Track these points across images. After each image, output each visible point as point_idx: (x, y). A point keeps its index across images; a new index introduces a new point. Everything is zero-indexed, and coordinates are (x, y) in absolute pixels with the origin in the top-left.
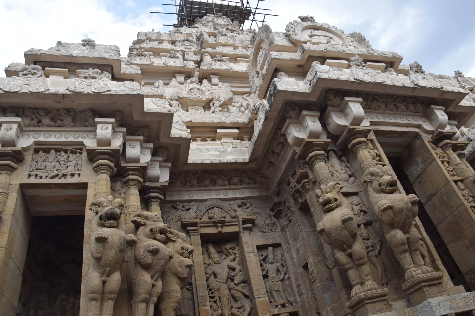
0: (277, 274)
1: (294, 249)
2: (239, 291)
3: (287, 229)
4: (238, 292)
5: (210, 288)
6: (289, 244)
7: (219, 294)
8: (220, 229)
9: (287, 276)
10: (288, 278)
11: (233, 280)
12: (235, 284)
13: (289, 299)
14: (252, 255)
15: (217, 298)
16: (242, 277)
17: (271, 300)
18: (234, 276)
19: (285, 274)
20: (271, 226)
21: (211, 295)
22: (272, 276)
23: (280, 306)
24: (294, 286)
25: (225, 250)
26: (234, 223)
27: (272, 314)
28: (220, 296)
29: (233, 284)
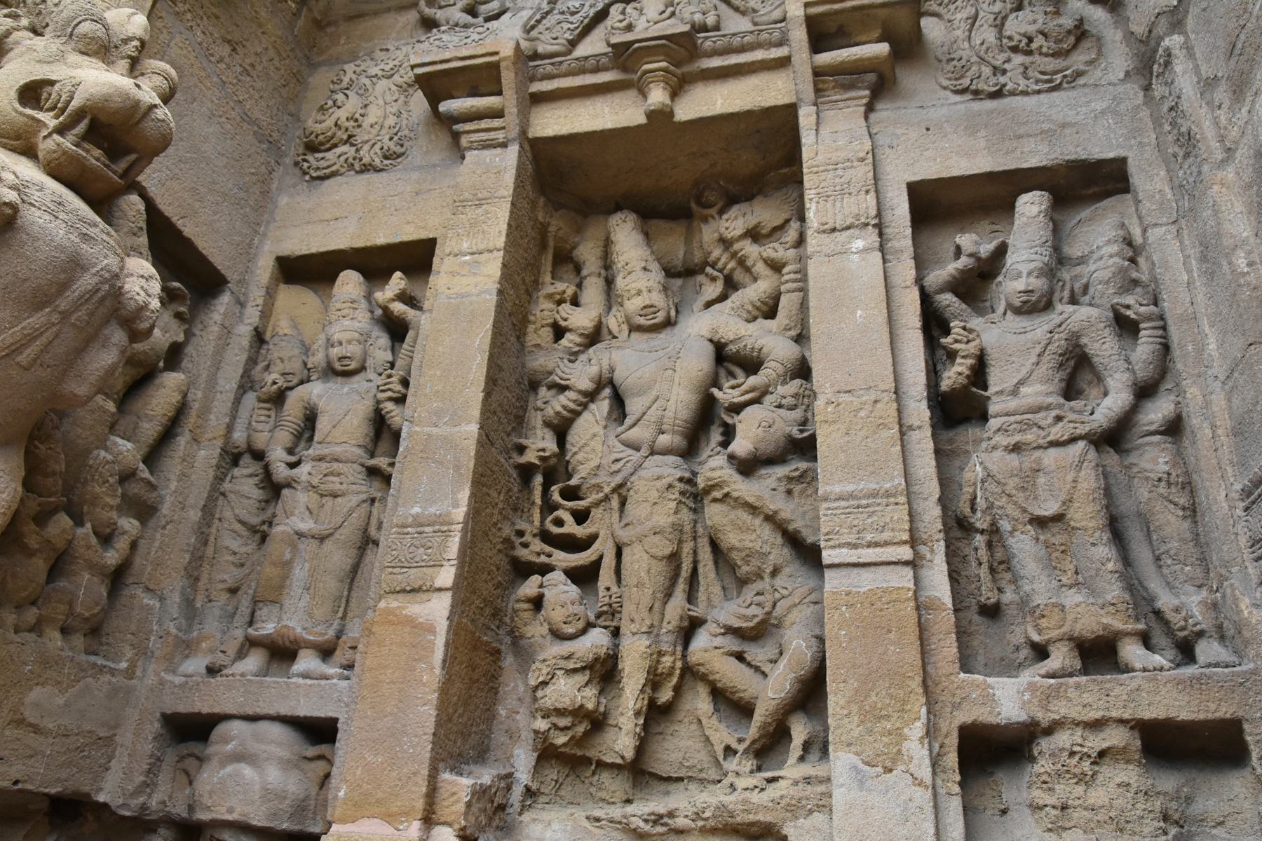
0: (1070, 391)
1: (1229, 174)
2: (753, 509)
3: (1173, 41)
4: (744, 516)
5: (574, 482)
6: (1188, 141)
7: (616, 526)
8: (658, 96)
9: (1157, 412)
10: (1174, 428)
11: (729, 433)
12: (731, 457)
13: (1165, 601)
14: (859, 244)
15: (603, 547)
16: (798, 414)
17: (988, 595)
18: (737, 409)
19: (1144, 392)
20: (1047, 46)
21: (570, 527)
22: (1013, 404)
23: (1060, 657)
24: (1221, 494)
25: (716, 253)
26: (759, 55)
27: (966, 716)
28: (624, 535)
29: (720, 460)
